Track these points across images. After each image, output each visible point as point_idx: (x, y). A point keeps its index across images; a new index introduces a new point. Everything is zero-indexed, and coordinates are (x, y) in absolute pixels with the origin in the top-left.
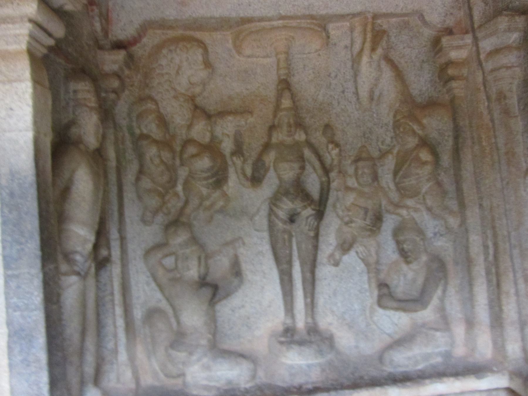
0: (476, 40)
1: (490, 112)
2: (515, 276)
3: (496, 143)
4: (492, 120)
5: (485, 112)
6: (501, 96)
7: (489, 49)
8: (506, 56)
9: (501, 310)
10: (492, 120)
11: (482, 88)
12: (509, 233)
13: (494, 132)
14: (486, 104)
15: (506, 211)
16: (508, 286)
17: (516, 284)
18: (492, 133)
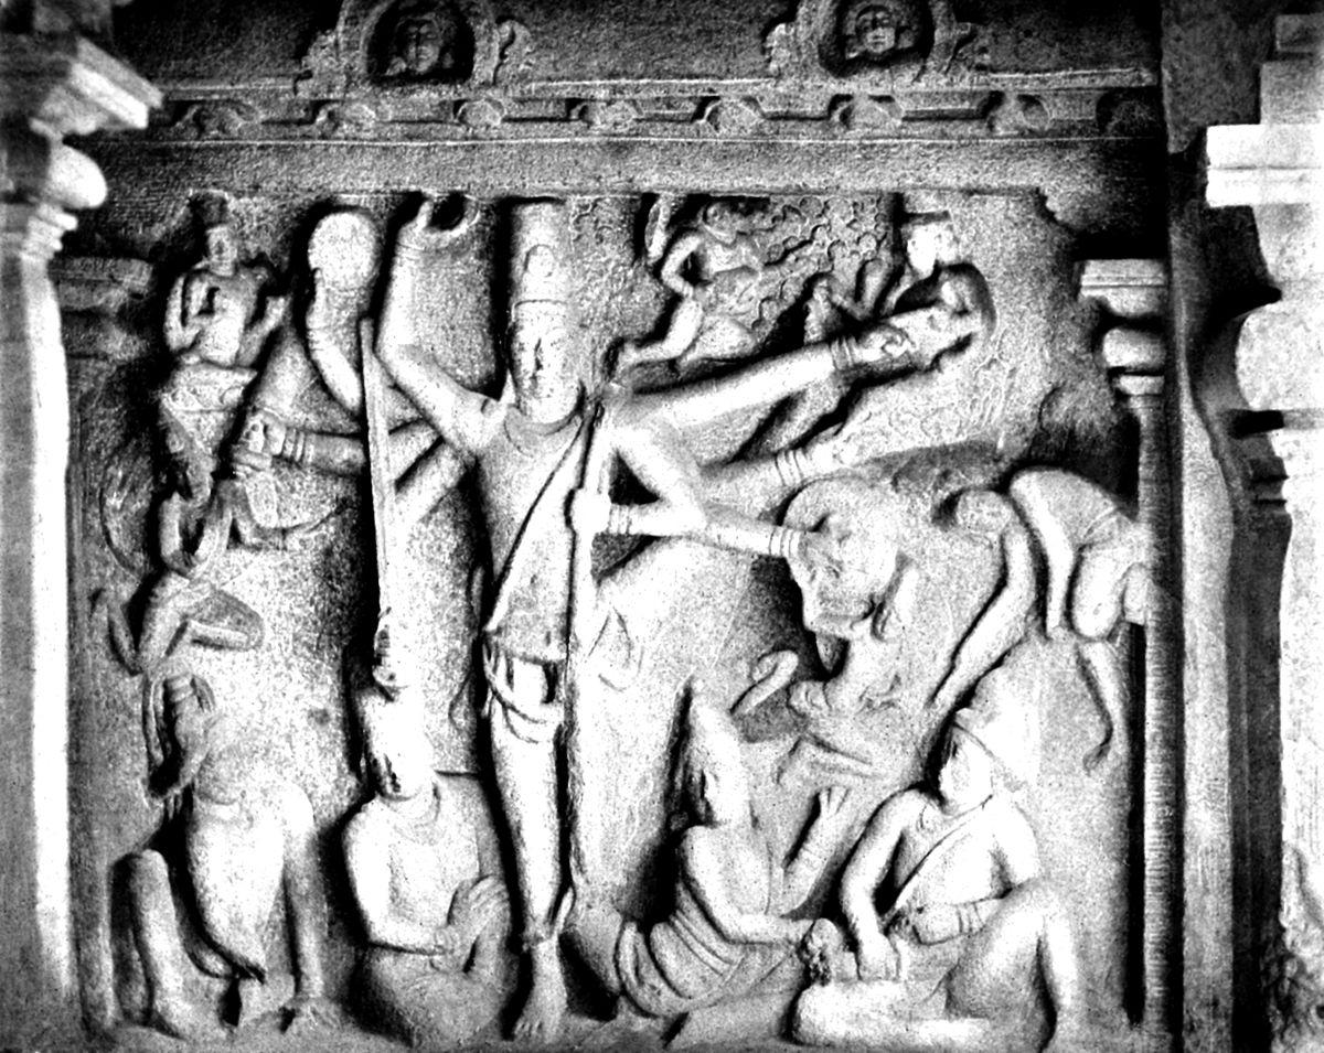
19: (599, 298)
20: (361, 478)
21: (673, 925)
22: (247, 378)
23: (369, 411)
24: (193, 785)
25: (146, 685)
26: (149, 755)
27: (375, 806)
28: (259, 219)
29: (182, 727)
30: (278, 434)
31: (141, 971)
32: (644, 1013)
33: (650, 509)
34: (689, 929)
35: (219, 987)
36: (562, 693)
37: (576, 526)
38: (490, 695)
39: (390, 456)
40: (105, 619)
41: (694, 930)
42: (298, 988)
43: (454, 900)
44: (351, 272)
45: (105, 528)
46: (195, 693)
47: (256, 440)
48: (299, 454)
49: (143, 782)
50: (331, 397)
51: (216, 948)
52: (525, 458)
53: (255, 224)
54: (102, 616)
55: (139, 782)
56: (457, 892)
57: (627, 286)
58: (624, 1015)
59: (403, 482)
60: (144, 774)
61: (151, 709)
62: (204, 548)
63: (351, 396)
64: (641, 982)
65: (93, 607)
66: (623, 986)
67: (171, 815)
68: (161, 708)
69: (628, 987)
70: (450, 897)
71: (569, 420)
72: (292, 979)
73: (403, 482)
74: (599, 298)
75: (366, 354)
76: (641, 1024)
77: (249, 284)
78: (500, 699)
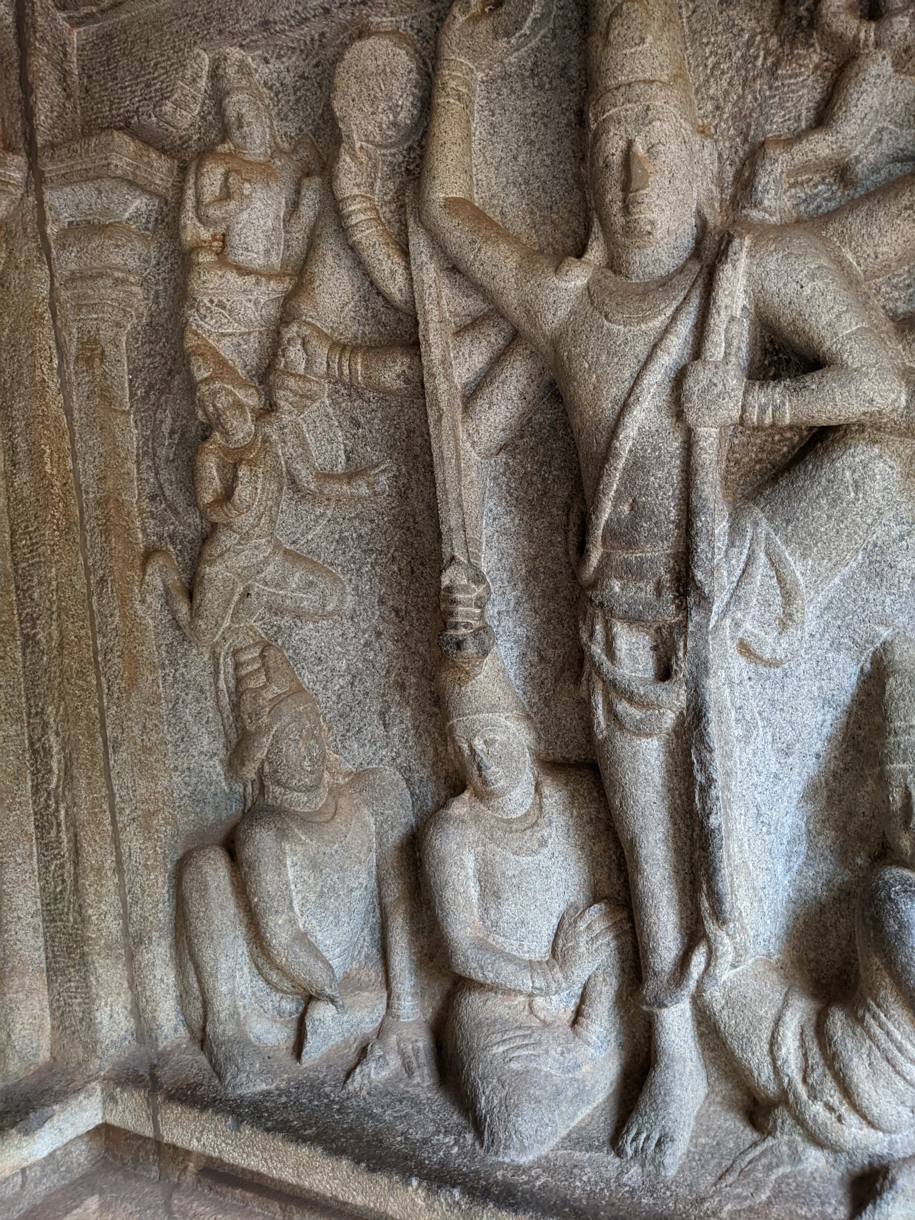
0: (36, 179)
1: (64, 388)
2: (114, 823)
3: (74, 471)
4: (68, 411)
5: (54, 384)
6: (92, 352)
7: (66, 217)
8: (117, 246)
9: (85, 921)
10: (68, 411)
11: (47, 315)
12: (102, 711)
13: (73, 442)
14: (56, 361)
15: (96, 653)
16: (96, 853)
17: (116, 841)
18: (67, 445)
19: (726, 93)
20: (418, 390)
21: (861, 1021)
22: (287, 284)
23: (417, 305)
24: (262, 768)
25: (215, 657)
26: (226, 735)
27: (460, 807)
28: (295, 94)
29: (247, 707)
30: (322, 352)
31: (196, 986)
32: (816, 1139)
33: (812, 381)
34: (888, 1033)
35: (289, 1006)
36: (683, 666)
37: (691, 417)
38: (587, 667)
39: (456, 361)
40: (158, 582)
41: (898, 1035)
42: (388, 1006)
43: (560, 925)
44: (385, 119)
45: (158, 480)
46: (263, 665)
47: (295, 354)
48: (346, 371)
49: (221, 761)
50: (388, 301)
51: (279, 968)
52: (615, 327)
53: (293, 98)
54: (155, 578)
55: (217, 762)
56: (563, 917)
57: (770, 60)
58: (785, 1138)
59: (472, 395)
60: (222, 754)
61: (222, 684)
62: (243, 492)
63: (395, 287)
64: (814, 1096)
65: (144, 571)
66: (785, 1092)
67: (249, 803)
68: (232, 683)
69: (791, 1096)
70: (555, 921)
71: (681, 270)
72: (385, 995)
73: (472, 395)
74: (726, 93)
75: (411, 223)
76: (815, 1160)
77: (286, 168)
78: (599, 673)
